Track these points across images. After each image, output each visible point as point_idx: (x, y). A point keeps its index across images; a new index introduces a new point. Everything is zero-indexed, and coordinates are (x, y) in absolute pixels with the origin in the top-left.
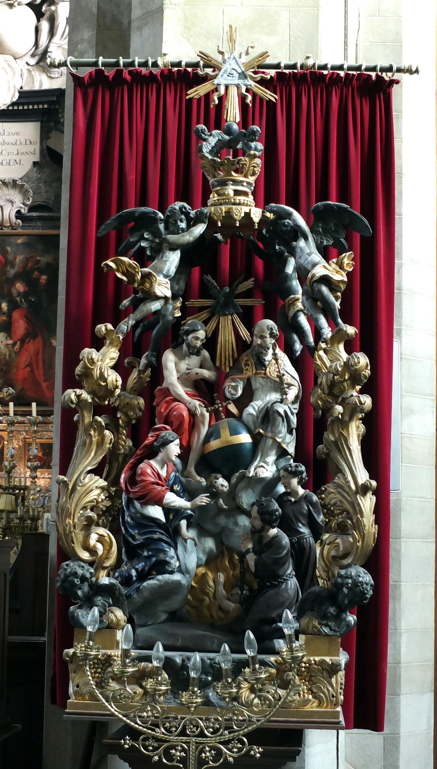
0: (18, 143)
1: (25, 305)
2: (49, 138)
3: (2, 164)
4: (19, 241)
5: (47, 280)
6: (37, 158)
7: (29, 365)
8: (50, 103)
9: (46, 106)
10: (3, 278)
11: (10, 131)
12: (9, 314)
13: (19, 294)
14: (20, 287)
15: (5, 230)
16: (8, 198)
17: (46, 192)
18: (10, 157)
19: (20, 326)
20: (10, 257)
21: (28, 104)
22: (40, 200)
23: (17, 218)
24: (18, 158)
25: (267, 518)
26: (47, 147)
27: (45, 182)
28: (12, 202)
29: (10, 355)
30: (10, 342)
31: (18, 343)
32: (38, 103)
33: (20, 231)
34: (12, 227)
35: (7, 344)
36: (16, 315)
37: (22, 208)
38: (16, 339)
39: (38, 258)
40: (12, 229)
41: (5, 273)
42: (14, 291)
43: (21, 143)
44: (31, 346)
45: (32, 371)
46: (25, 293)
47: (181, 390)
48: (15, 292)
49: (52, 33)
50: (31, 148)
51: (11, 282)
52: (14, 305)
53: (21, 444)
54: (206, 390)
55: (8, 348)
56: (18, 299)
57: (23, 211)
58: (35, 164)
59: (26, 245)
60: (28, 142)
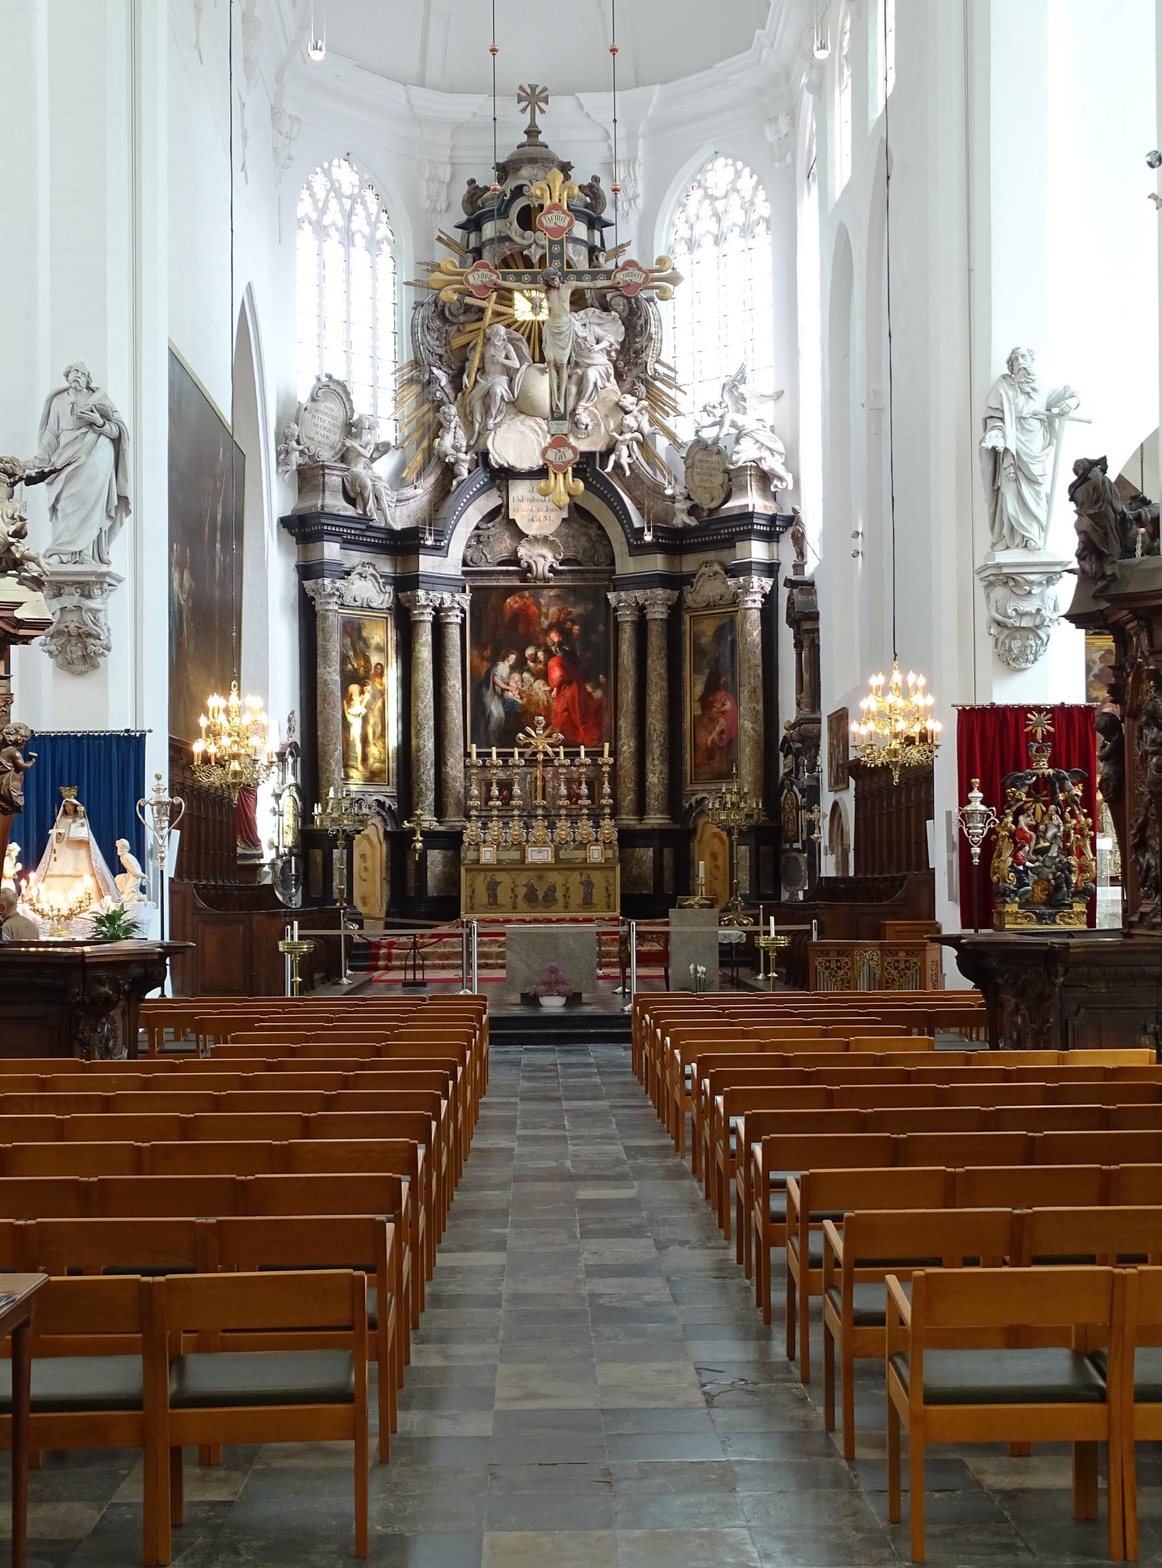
1: (560, 654)
4: (552, 593)
6: (565, 515)
7: (566, 710)
14: (554, 637)
15: (539, 583)
16: (540, 552)
19: (556, 674)
20: (544, 610)
22: (570, 554)
25: (1058, 869)
28: (544, 557)
33: (552, 583)
36: (552, 663)
41: (540, 624)
44: (568, 693)
45: (569, 715)
46: (559, 642)
47: (1026, 829)
49: (580, 394)
51: (547, 632)
52: (549, 654)
54: (1034, 828)
59: (557, 596)
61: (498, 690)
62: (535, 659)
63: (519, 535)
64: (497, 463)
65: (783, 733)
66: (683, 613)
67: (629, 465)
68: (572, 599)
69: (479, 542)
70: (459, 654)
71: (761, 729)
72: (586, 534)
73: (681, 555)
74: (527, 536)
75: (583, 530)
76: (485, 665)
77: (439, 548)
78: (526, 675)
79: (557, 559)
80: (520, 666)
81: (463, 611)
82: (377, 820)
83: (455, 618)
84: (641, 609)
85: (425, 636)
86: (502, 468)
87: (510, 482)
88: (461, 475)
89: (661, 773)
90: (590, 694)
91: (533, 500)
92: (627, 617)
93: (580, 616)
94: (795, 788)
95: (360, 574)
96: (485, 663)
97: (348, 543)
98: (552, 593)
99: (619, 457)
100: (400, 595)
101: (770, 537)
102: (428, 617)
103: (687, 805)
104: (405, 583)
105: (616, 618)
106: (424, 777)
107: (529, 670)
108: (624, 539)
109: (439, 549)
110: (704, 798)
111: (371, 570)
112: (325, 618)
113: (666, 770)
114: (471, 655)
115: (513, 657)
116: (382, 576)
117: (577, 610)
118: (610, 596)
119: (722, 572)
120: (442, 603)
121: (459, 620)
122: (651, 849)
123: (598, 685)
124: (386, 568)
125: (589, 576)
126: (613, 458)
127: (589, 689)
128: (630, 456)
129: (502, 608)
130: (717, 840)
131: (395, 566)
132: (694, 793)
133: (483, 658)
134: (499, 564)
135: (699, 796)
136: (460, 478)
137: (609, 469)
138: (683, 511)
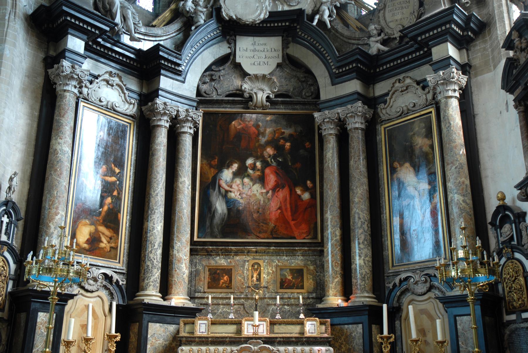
0: (266, 50)
1: (274, 164)
2: (288, 48)
3: (254, 64)
5: (291, 146)
6: (280, 60)
7: (280, 208)
8: (292, 21)
9: (287, 24)
10: (257, 144)
11: (259, 42)
12: (263, 171)
13: (270, 156)
14: (270, 151)
17: (287, 85)
18: (260, 60)
19: (272, 179)
20: (262, 130)
21: (274, 22)
22: (283, 91)
23: (267, 101)
24: (266, 61)
26: (287, 54)
27: (285, 78)
28: (263, 90)
29: (264, 201)
30: (264, 191)
31: (270, 192)
32: (281, 21)
34: (263, 107)
35: (262, 193)
36: (267, 171)
37: (270, 94)
38: (268, 189)
39: (283, 131)
40: (263, 109)
41: (258, 141)
42: (266, 154)
43: (268, 51)
45: (282, 213)
48: (267, 154)
50: (275, 54)
51: (263, 147)
52: (266, 164)
53: (274, 269)
55: (262, 195)
56: (269, 159)
57: (271, 96)
58: (279, 65)
60: (273, 50)
61: (223, 191)
62: (254, 167)
63: (244, 74)
64: (227, 15)
65: (492, 205)
66: (378, 127)
67: (330, 21)
68: (285, 123)
69: (212, 80)
70: (190, 158)
71: (470, 201)
72: (296, 76)
73: (374, 84)
74: (250, 75)
75: (294, 73)
76: (211, 173)
77: (178, 73)
78: (246, 180)
79: (273, 92)
80: (241, 173)
81: (196, 127)
82: (103, 293)
83: (188, 129)
84: (341, 125)
85: (162, 139)
86: (231, 18)
87: (238, 37)
88: (199, 21)
89: (366, 256)
90: (299, 196)
91: (255, 50)
92: (330, 132)
93: (291, 135)
94: (518, 255)
95: (107, 82)
96: (212, 170)
97: (94, 50)
98: (268, 118)
99: (322, 16)
100: (143, 108)
101: (462, 43)
102: (165, 123)
103: (391, 286)
104: (148, 97)
105: (320, 135)
106: (151, 256)
107: (248, 176)
108: (327, 74)
109: (176, 71)
110: (407, 279)
111: (116, 80)
112: (63, 97)
113: (370, 253)
114: (201, 161)
115: (235, 166)
116: (127, 89)
117: (288, 131)
118: (316, 115)
119: (415, 84)
120: (177, 116)
121: (192, 131)
122: (360, 326)
123: (306, 189)
124: (134, 86)
125: (298, 107)
126: (317, 17)
127: (299, 192)
128: (330, 16)
129: (228, 129)
130: (424, 317)
131: (141, 87)
132: (397, 274)
133: (211, 166)
134: (227, 96)
135: (403, 276)
136: (199, 23)
137: (315, 23)
138: (377, 42)
